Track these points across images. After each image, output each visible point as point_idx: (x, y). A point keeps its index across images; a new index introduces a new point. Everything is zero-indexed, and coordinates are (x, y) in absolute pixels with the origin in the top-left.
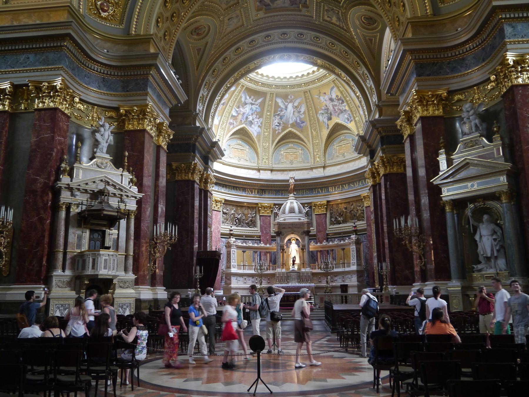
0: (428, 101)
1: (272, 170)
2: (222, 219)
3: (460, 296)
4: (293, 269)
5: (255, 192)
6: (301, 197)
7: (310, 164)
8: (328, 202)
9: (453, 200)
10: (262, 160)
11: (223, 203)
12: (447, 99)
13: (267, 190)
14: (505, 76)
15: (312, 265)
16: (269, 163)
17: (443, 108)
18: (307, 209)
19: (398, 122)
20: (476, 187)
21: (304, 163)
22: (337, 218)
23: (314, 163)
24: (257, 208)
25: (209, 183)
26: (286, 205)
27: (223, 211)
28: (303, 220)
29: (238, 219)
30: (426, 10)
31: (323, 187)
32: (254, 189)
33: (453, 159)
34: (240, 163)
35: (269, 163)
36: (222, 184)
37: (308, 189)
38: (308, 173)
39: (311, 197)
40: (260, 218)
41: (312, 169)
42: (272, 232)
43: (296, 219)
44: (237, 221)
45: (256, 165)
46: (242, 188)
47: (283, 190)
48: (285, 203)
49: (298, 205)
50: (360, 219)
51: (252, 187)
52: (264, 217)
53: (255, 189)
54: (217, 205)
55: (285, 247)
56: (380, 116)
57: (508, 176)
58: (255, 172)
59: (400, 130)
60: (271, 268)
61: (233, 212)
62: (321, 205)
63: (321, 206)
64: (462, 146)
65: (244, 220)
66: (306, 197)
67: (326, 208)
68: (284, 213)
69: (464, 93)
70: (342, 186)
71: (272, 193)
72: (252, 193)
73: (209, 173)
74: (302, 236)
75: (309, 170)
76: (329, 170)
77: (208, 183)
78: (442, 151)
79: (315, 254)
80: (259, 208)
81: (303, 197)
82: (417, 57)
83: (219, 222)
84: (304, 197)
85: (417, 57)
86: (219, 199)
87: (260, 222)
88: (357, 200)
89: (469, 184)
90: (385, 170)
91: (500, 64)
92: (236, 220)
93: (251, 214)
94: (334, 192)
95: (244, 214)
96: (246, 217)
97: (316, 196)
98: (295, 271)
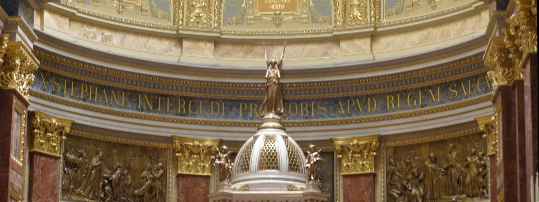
1: (217, 42)
2: (60, 183)
5: (164, 104)
6: (303, 124)
7: (331, 27)
8: (381, 139)
10: (190, 11)
11: (66, 135)
13: (201, 99)
16: (209, 19)
18: (314, 157)
21: (314, 21)
22: (405, 189)
23: (344, 23)
24: (169, 153)
25: (18, 70)
26: (252, 143)
27: (65, 158)
28: (302, 189)
29: (110, 182)
31: (367, 96)
32: (162, 95)
34: (123, 17)
35: (209, 19)
36: (65, 78)
37: (323, 100)
38: (326, 54)
39: (332, 123)
40: (178, 184)
41: (336, 40)
43: (280, 186)
44: (107, 188)
45: (170, 24)
46: (126, 91)
47: (248, 102)
48: (251, 139)
49: (288, 144)
50: (475, 191)
51: (156, 91)
52: (189, 180)
53: (165, 96)
54: (48, 140)
58: (166, 44)
61: (95, 161)
62: (360, 150)
63: (361, 153)
65: (129, 186)
66: (317, 124)
67: (376, 158)
68: (246, 167)
70: (424, 93)
71: (216, 110)
72: (155, 106)
73: (18, 38)
75: (330, 44)
76: (388, 45)
77: (13, 69)
80: (175, 151)
81: (308, 124)
83: (54, 188)
84: (313, 124)
86: (54, 121)
87: (179, 195)
88: (467, 136)
92: (104, 185)
93: (150, 169)
94: (401, 109)
95: (129, 169)
96: (134, 178)
97: (346, 123)
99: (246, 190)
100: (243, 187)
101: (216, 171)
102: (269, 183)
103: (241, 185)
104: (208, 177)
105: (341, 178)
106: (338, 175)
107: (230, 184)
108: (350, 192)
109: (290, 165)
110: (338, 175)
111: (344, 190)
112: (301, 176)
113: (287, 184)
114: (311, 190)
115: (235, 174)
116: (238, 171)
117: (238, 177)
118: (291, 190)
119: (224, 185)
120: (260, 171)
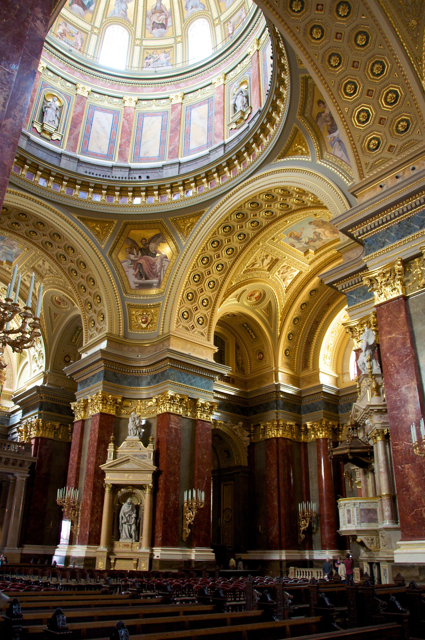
0: (107, 402)
3: (105, 559)
9: (113, 484)
12: (121, 404)
14: (163, 404)
17: (116, 411)
19: (73, 405)
20: (130, 477)
30: (120, 331)
33: (117, 452)
56: (44, 382)
57: (153, 474)
59: (73, 411)
64: (126, 445)
69: (131, 402)
78: (111, 445)
82: (108, 366)
85: (108, 366)
89: (126, 475)
90: (38, 433)
91: (162, 394)
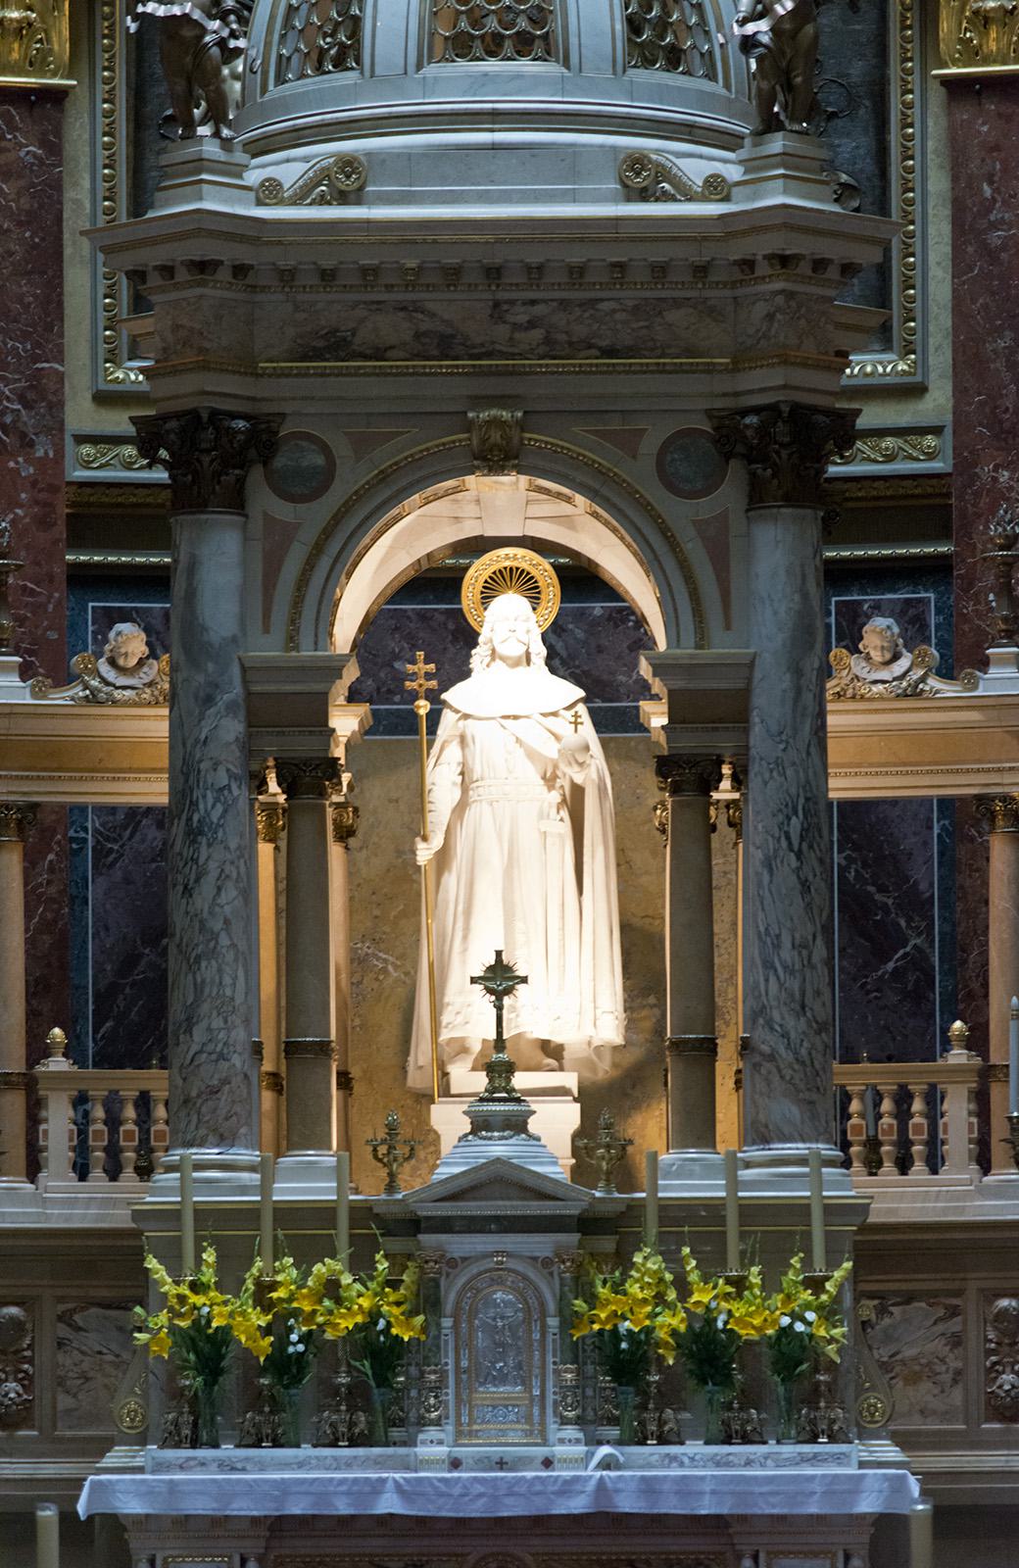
4: (499, 1148)
15: (856, 1076)
28: (715, 187)
42: (81, 414)
43: (569, 163)
55: (345, 722)
60: (58, 1123)
74: (706, 507)
79: (929, 876)
98: (536, 1189)
99: (343, 198)
100: (323, 176)
101: (102, 58)
102: (495, 147)
103: (306, 159)
104: (57, 96)
105: (937, 96)
106: (915, 80)
107: (240, 157)
108: (997, 190)
109: (634, 25)
110: (915, 80)
111: (955, 179)
112: (705, 100)
113: (614, 149)
114: (775, 197)
115: (264, 90)
116: (283, 62)
117: (284, 105)
118: (644, 195)
119: (200, 164)
120: (431, 70)
